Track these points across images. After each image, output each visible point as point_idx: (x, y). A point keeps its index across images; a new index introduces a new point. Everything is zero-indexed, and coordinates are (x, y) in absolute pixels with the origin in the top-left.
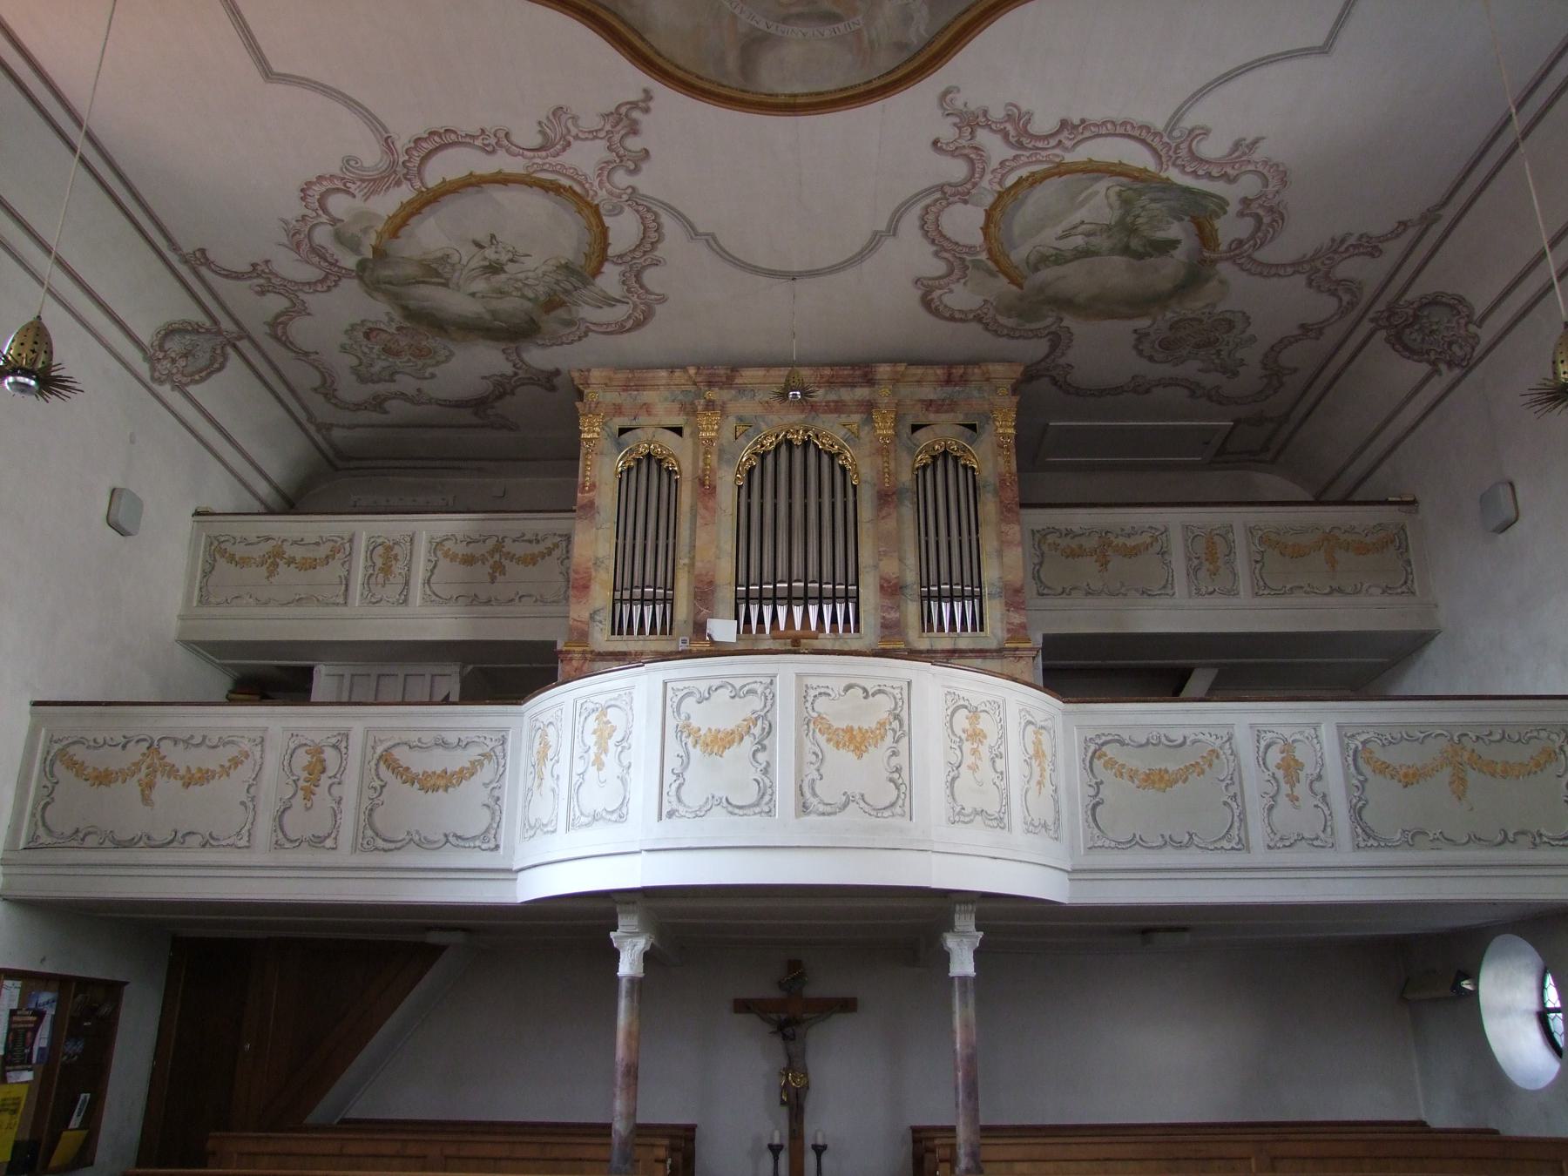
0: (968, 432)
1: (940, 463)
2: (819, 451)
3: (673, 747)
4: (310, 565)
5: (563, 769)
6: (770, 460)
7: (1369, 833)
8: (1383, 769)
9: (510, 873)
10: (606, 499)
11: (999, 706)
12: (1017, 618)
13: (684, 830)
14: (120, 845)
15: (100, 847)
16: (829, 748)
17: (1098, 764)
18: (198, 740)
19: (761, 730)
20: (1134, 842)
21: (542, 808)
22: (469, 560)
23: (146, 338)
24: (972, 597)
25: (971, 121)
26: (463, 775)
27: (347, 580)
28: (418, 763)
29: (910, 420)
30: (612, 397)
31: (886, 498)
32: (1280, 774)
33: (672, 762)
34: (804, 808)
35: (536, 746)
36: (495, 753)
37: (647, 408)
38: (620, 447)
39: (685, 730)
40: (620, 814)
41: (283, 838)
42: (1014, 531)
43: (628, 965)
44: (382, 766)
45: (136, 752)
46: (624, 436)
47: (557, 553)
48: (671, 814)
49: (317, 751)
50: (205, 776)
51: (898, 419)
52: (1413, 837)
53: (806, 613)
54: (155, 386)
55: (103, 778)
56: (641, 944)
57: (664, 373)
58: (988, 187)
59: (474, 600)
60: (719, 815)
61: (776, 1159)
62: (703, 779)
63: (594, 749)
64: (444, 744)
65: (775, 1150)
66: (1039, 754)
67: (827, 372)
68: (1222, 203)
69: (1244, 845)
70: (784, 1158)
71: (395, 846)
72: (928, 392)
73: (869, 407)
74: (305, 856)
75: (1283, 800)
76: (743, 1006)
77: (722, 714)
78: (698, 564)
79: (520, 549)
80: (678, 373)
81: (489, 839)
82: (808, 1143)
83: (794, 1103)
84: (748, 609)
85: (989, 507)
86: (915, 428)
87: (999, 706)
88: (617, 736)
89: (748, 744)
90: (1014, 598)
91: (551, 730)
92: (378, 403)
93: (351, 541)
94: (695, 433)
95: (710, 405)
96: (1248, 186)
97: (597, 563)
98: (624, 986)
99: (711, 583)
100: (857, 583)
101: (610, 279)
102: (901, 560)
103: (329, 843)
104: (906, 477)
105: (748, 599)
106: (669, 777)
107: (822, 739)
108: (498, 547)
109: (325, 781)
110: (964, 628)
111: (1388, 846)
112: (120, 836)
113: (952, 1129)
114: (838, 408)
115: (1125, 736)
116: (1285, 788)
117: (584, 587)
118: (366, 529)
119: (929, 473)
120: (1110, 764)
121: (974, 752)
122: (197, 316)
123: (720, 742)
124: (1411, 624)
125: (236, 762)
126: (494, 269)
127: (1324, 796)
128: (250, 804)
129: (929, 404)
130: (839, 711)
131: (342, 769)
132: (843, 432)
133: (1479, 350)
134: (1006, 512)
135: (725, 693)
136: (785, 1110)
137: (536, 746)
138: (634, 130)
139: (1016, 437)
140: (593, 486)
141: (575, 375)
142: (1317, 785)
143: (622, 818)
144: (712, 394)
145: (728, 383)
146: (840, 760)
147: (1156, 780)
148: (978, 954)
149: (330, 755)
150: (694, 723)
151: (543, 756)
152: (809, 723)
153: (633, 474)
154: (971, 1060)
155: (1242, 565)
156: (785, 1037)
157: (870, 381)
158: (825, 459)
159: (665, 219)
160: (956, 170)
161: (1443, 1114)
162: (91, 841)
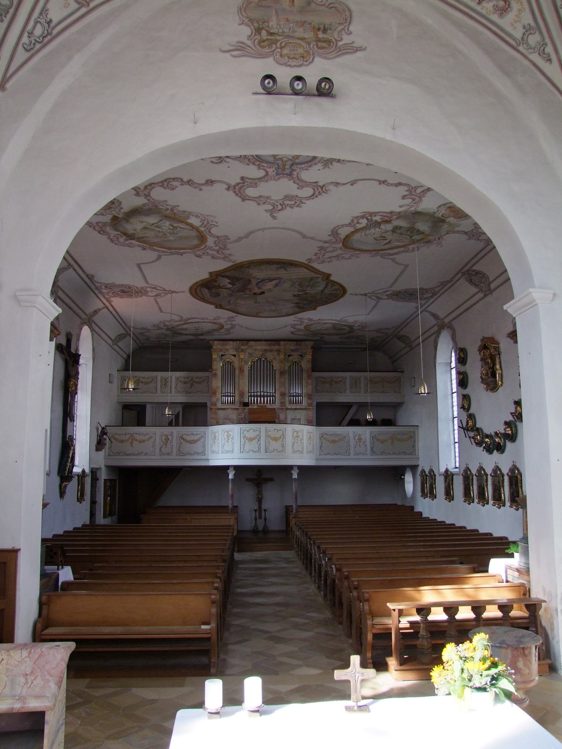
0: (301, 357)
1: (294, 364)
2: (267, 361)
3: (242, 440)
4: (147, 383)
5: (220, 441)
6: (256, 363)
7: (374, 452)
8: (378, 440)
9: (208, 460)
10: (219, 373)
11: (302, 430)
12: (310, 401)
13: (244, 455)
14: (127, 455)
15: (123, 455)
16: (271, 441)
17: (322, 438)
18: (141, 433)
19: (258, 438)
20: (329, 454)
21: (215, 448)
22: (185, 383)
23: (113, 338)
24: (300, 396)
25: (302, 319)
26: (197, 441)
27: (156, 387)
28: (188, 438)
29: (288, 354)
30: (219, 347)
31: (282, 373)
32: (357, 441)
33: (242, 443)
34: (266, 452)
35: (213, 436)
36: (203, 436)
37: (227, 350)
38: (221, 359)
39: (244, 437)
40: (232, 451)
41: (162, 454)
42: (310, 381)
43: (231, 476)
44: (181, 439)
45: (128, 437)
46: (223, 357)
47: (206, 381)
48: (242, 452)
49: (167, 436)
50: (144, 441)
51: (285, 355)
52: (382, 453)
53: (264, 399)
54: (113, 347)
55: (122, 441)
56: (234, 472)
57: (231, 342)
58: (305, 324)
59: (187, 392)
60: (251, 453)
61: (256, 512)
62: (248, 446)
63: (226, 439)
64: (193, 434)
65: (256, 511)
66: (310, 437)
67: (269, 342)
68: (355, 326)
69: (349, 454)
70: (257, 512)
71: (184, 454)
72: (293, 347)
73: (279, 351)
74: (166, 457)
75: (357, 446)
76: (248, 480)
77: (251, 434)
78: (240, 388)
79: (197, 380)
80: (235, 342)
81: (203, 453)
82: (263, 509)
83: (260, 501)
84: (251, 398)
85: (305, 376)
86: (289, 356)
87: (302, 430)
88: (231, 437)
89: (256, 440)
90: (309, 397)
91: (216, 433)
92: (159, 341)
93: (156, 377)
94: (239, 357)
95: (242, 350)
96: (358, 324)
97: (217, 387)
98: (230, 481)
99: (243, 393)
100: (275, 393)
101: (223, 330)
102: (285, 388)
103: (171, 454)
104: (287, 368)
105: (251, 396)
106: (242, 446)
107: (269, 439)
108: (192, 380)
109: (169, 442)
110: (298, 403)
111: (378, 455)
112: (128, 453)
113: (292, 506)
114: (271, 351)
115: (328, 433)
116: (358, 444)
117: (215, 393)
118: (160, 375)
119: (292, 366)
120: (325, 438)
121: (297, 440)
122: (125, 333)
123: (251, 440)
124: (399, 401)
125: (150, 438)
126: (197, 329)
127: (366, 446)
128: (154, 446)
129: (292, 350)
130: (273, 434)
131: (172, 440)
132: (272, 357)
133: (413, 347)
134: (309, 377)
135: (252, 431)
136: (257, 503)
137: (213, 436)
138: (234, 318)
139: (312, 359)
140: (216, 370)
141: (211, 342)
142: (365, 443)
143: (233, 452)
144: (242, 347)
145: (247, 344)
146: (273, 443)
147: (333, 442)
148: (298, 474)
149: (170, 437)
150: (246, 436)
151: (215, 438)
152: (268, 436)
153: (225, 366)
154: (296, 493)
155: (362, 385)
156: (258, 487)
157: (279, 345)
158: (268, 362)
159: (236, 326)
160: (299, 323)
161: (399, 503)
162: (121, 454)
